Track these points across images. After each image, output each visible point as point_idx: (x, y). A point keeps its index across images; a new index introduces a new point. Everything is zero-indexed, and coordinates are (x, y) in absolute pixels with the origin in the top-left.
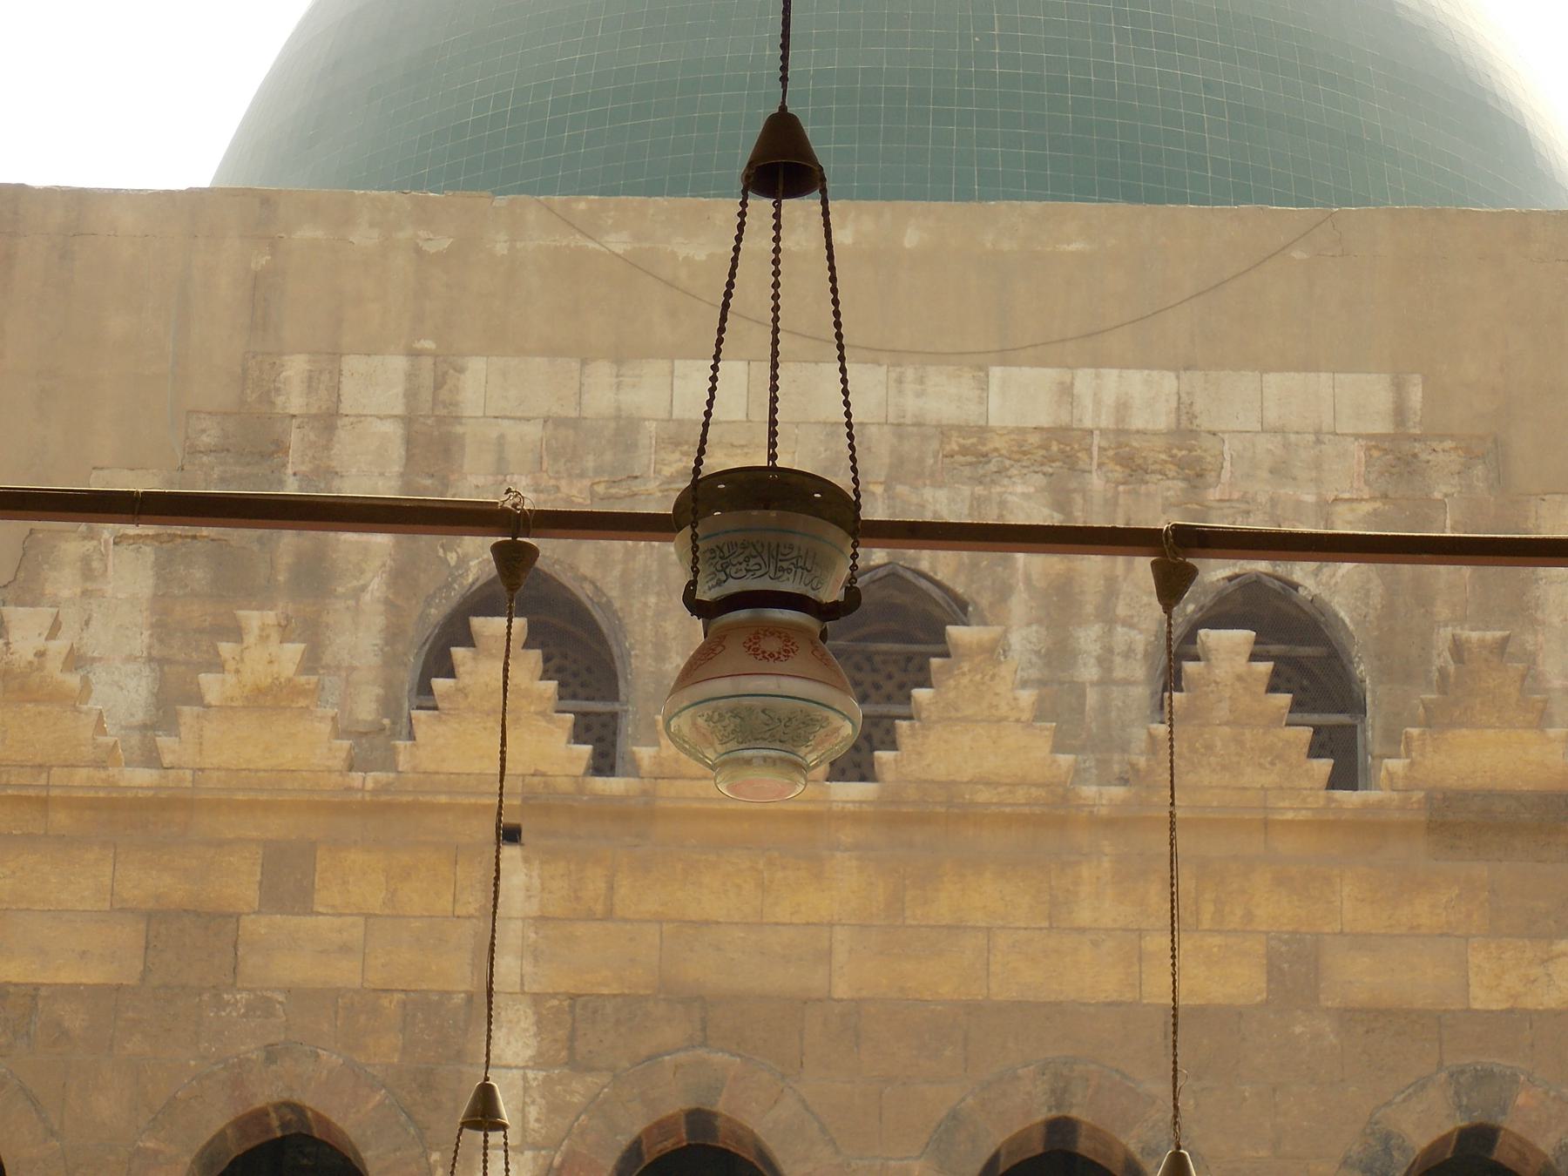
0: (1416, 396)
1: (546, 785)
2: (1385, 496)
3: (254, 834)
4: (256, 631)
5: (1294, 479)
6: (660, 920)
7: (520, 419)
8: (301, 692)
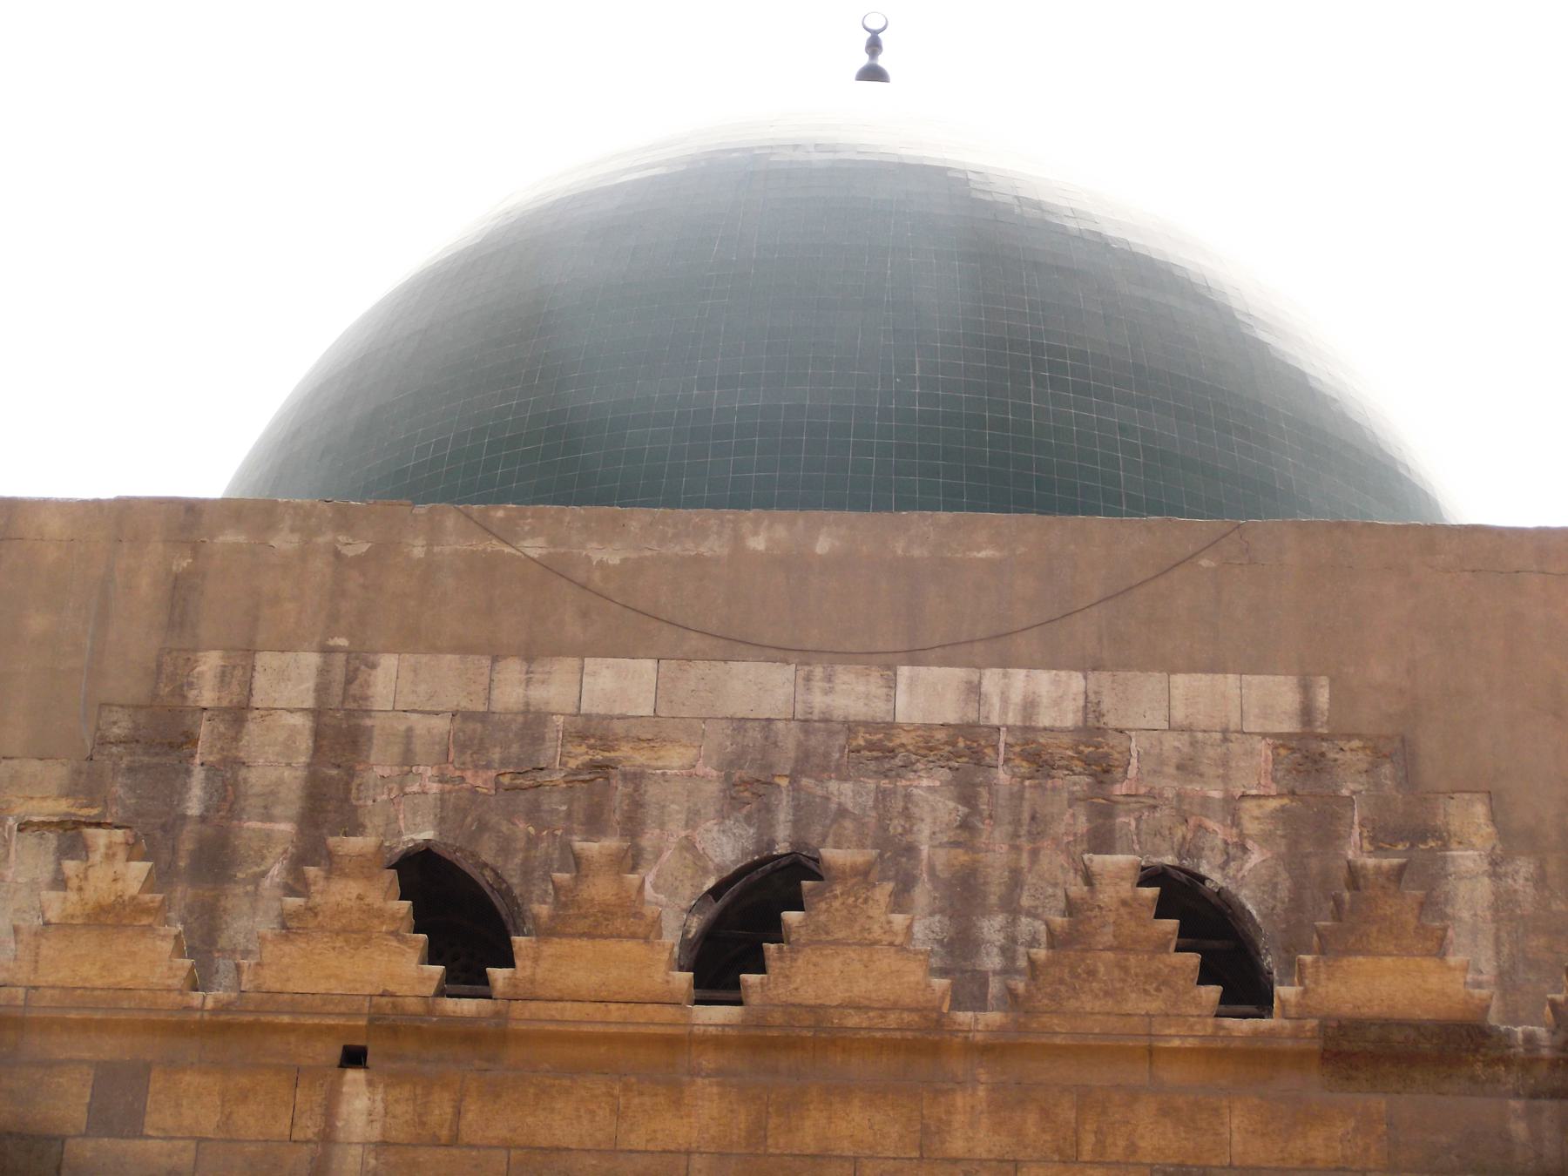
0: (1323, 697)
1: (394, 1006)
2: (1293, 793)
3: (86, 1055)
4: (102, 850)
5: (1201, 775)
6: (507, 1146)
7: (429, 713)
8: (146, 910)
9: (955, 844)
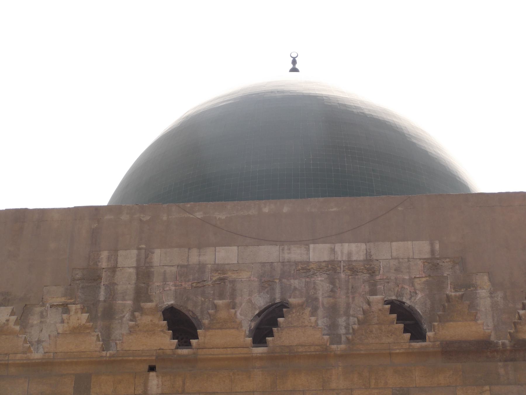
0: (437, 247)
2: (430, 276)
4: (74, 311)
5: (402, 272)
7: (171, 266)
9: (330, 297)
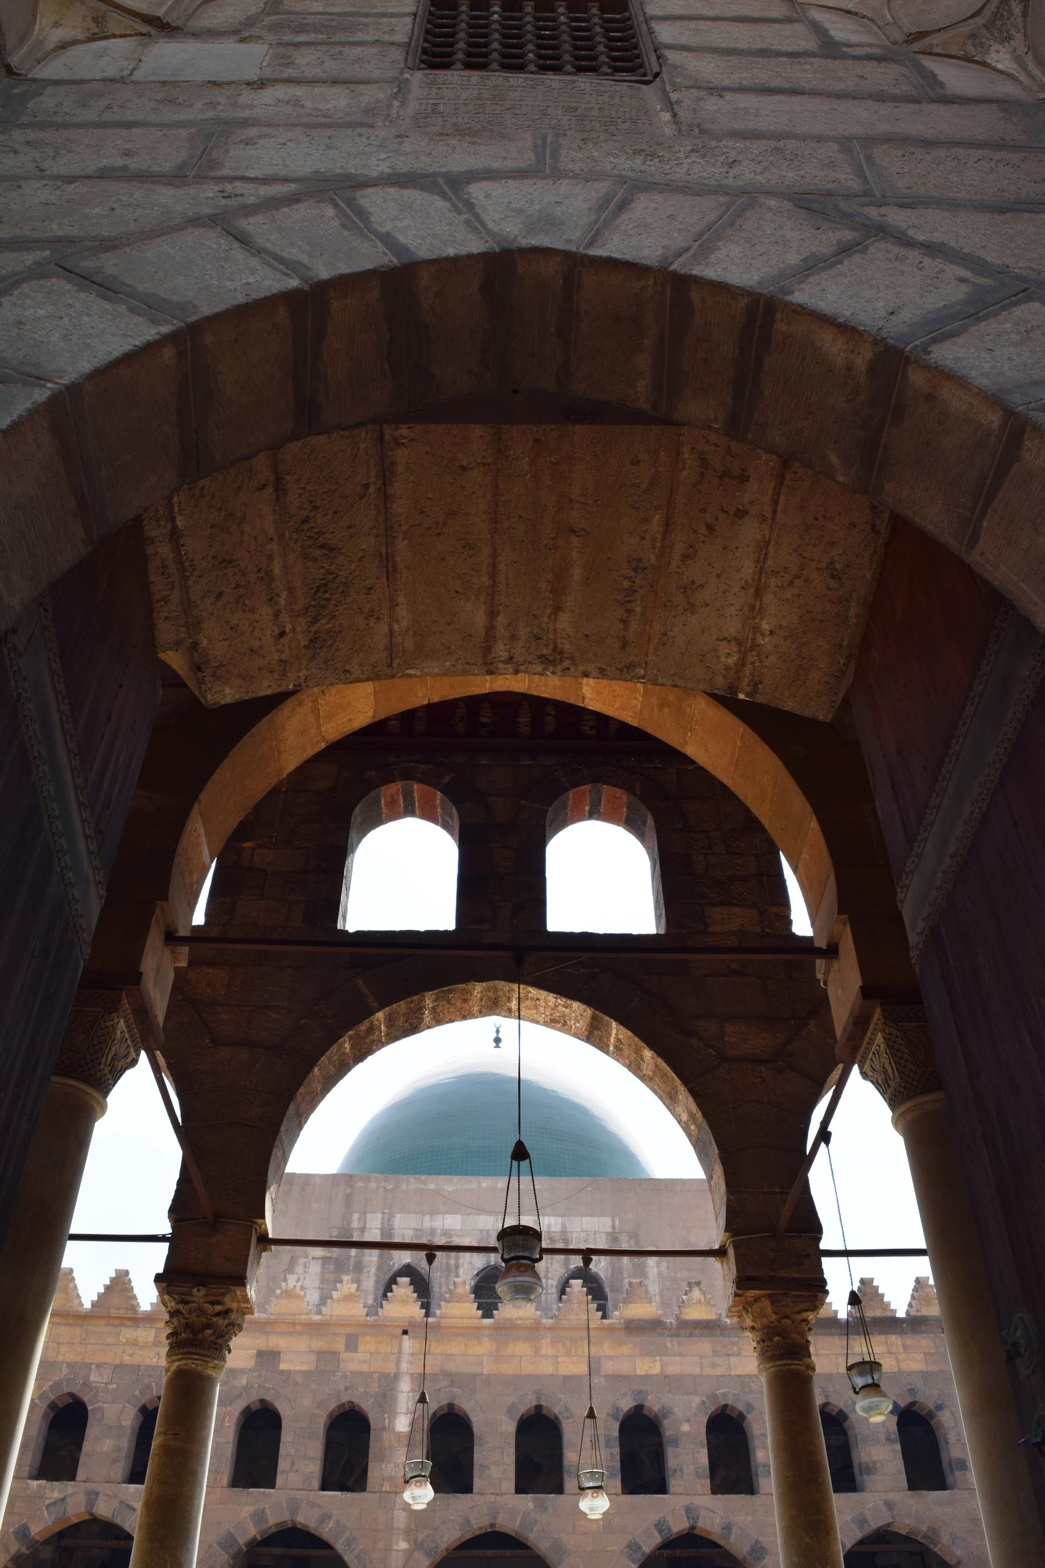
0: (617, 1223)
